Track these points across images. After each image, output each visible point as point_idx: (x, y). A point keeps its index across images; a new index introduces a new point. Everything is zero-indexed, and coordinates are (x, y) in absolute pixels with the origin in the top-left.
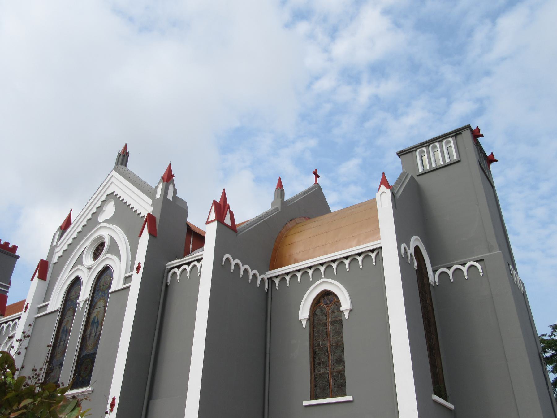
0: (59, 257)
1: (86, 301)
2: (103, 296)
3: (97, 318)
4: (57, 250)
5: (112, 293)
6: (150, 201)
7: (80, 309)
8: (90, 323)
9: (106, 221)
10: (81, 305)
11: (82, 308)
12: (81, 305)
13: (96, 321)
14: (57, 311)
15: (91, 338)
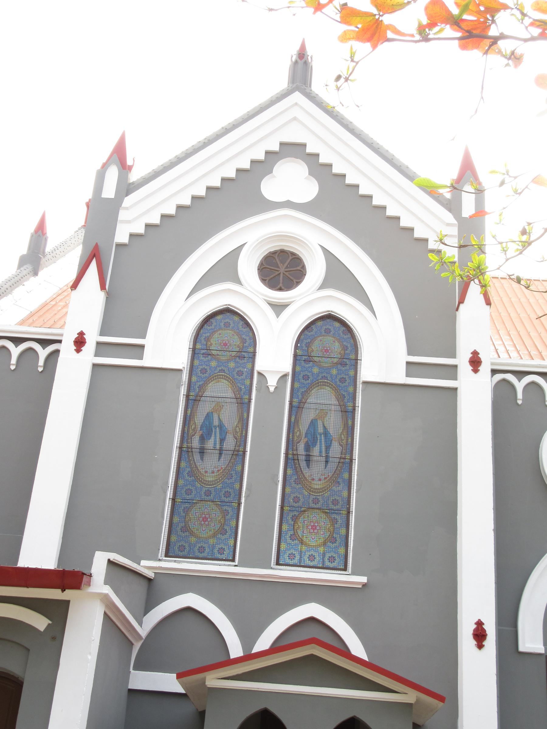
0: (132, 235)
1: (285, 376)
2: (326, 378)
3: (324, 427)
4: (123, 215)
5: (365, 383)
6: (449, 217)
7: (272, 389)
8: (304, 431)
9: (288, 204)
10: (272, 382)
11: (276, 388)
12: (272, 382)
13: (320, 430)
14: (180, 371)
15: (313, 465)
